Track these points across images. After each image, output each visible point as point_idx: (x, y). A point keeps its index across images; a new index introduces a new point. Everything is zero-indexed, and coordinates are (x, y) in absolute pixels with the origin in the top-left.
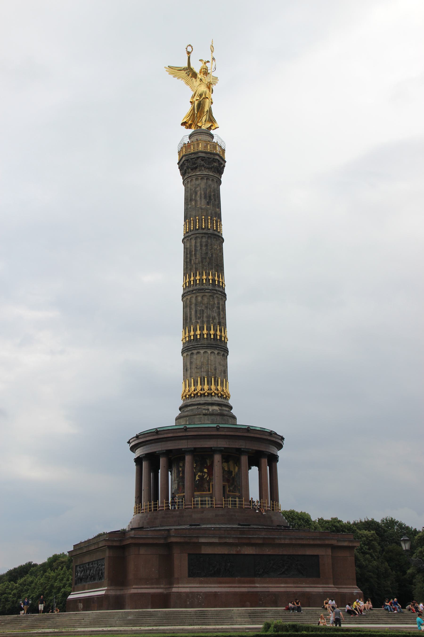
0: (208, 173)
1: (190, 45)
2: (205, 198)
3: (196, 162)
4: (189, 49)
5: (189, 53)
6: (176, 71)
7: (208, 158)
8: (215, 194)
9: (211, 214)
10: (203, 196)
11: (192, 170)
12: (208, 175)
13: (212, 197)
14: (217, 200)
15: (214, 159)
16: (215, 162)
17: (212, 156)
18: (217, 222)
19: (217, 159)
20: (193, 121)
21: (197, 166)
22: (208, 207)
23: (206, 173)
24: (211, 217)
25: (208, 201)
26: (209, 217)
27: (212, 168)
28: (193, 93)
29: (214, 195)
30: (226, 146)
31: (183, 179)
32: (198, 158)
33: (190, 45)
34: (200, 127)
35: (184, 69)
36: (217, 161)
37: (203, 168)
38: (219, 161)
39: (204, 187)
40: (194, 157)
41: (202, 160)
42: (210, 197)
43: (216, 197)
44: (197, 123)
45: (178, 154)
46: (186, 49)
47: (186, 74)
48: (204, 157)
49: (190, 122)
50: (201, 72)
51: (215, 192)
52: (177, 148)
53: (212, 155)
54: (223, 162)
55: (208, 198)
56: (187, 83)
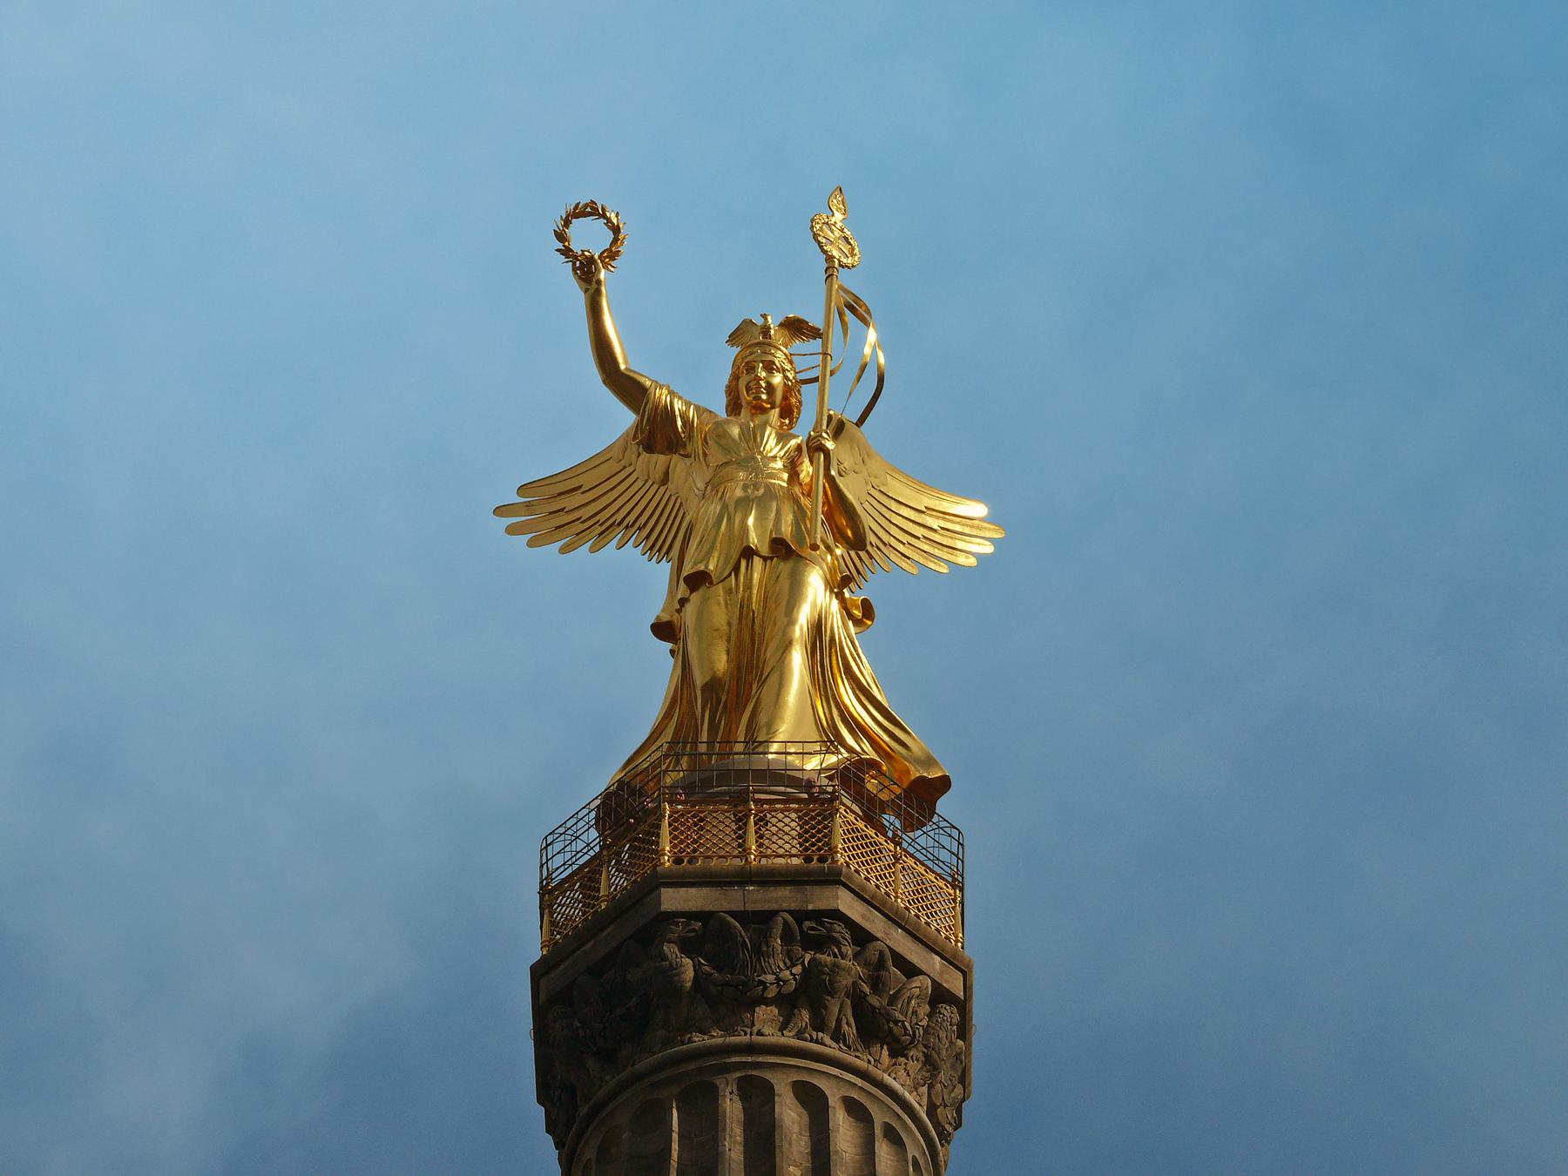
1: (590, 210)
4: (589, 237)
5: (586, 270)
12: (751, 1049)
15: (800, 916)
19: (837, 915)
33: (590, 210)
36: (839, 927)
38: (862, 937)
46: (561, 236)
48: (704, 916)
50: (734, 407)
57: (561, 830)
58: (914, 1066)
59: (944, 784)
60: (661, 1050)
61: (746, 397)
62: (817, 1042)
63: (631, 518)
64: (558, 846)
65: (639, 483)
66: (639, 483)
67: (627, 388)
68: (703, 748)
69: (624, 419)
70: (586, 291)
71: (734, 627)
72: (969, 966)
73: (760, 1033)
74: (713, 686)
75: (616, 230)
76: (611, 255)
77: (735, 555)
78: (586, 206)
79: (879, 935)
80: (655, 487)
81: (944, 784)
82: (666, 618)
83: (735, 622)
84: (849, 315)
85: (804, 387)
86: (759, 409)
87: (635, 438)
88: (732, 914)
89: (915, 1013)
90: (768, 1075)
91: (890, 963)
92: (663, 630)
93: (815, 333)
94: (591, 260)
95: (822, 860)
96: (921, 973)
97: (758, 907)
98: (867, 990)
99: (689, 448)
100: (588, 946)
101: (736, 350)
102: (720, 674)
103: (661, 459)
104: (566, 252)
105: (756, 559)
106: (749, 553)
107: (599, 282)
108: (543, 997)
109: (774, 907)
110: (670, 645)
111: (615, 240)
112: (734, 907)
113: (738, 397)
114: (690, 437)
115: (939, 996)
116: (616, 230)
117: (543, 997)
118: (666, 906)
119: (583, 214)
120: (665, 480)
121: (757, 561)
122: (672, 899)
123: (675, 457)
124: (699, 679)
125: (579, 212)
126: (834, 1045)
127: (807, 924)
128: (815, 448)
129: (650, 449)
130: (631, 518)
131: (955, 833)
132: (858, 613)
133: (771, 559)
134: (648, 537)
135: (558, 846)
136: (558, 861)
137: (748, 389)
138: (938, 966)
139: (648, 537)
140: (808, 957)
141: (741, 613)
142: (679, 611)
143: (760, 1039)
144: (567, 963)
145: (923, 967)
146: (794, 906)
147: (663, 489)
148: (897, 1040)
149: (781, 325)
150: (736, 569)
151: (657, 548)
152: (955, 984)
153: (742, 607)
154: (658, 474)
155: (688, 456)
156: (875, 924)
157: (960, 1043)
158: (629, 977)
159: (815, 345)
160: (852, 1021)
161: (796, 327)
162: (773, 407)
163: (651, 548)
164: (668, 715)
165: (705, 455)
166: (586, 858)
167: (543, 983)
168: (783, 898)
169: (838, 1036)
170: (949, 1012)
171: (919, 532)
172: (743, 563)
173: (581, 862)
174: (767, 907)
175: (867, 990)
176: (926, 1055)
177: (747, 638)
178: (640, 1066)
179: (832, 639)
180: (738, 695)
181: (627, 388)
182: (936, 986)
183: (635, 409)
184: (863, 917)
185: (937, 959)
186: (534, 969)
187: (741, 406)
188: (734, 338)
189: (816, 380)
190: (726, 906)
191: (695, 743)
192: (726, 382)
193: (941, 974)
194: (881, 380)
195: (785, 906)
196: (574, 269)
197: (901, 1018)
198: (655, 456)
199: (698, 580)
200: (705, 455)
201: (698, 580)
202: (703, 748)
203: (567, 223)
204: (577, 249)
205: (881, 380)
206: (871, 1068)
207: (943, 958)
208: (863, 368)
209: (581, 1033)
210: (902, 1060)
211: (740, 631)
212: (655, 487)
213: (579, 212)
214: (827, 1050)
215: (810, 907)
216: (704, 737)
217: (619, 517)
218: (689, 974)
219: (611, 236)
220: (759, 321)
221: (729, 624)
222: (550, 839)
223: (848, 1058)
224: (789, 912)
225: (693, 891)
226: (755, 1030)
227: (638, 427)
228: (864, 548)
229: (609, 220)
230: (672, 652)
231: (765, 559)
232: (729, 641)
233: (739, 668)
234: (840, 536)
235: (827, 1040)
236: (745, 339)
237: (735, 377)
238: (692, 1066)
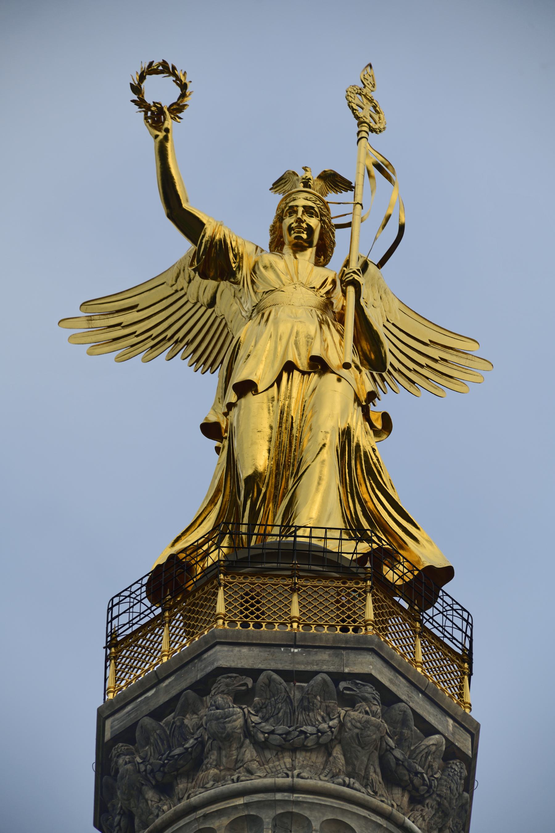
1: (165, 69)
3: (190, 721)
4: (160, 90)
5: (156, 117)
7: (289, 676)
11: (166, 789)
12: (292, 789)
15: (337, 677)
16: (350, 702)
21: (201, 743)
23: (268, 781)
27: (326, 749)
32: (202, 687)
36: (369, 690)
37: (249, 753)
38: (389, 699)
41: (241, 697)
46: (136, 89)
48: (254, 673)
50: (277, 245)
53: (325, 656)
57: (127, 593)
58: (428, 812)
59: (447, 573)
60: (213, 786)
61: (288, 238)
62: (348, 786)
63: (181, 334)
64: (124, 607)
65: (189, 306)
66: (189, 306)
67: (188, 224)
68: (244, 529)
69: (181, 247)
70: (156, 137)
71: (276, 429)
72: (477, 726)
73: (299, 776)
74: (254, 479)
75: (183, 87)
76: (177, 109)
77: (278, 366)
78: (160, 64)
79: (403, 697)
80: (203, 309)
81: (447, 573)
82: (213, 419)
83: (276, 426)
84: (375, 172)
85: (338, 232)
86: (299, 247)
87: (191, 265)
88: (277, 671)
89: (430, 767)
90: (307, 813)
91: (412, 723)
92: (210, 430)
93: (348, 186)
94: (161, 111)
95: (356, 630)
96: (437, 732)
97: (302, 668)
98: (392, 743)
99: (239, 276)
100: (150, 694)
101: (279, 197)
102: (261, 469)
103: (211, 284)
104: (141, 103)
105: (296, 373)
106: (289, 367)
107: (167, 130)
108: (108, 736)
109: (315, 668)
110: (216, 443)
111: (183, 96)
112: (280, 667)
113: (281, 236)
114: (239, 268)
115: (452, 753)
116: (183, 87)
117: (108, 736)
118: (223, 663)
119: (156, 72)
120: (212, 303)
121: (296, 373)
123: (224, 284)
124: (245, 472)
125: (151, 70)
126: (363, 790)
128: (348, 282)
129: (204, 276)
130: (181, 334)
131: (465, 615)
132: (379, 425)
133: (309, 374)
134: (194, 351)
135: (124, 607)
136: (124, 619)
137: (290, 229)
138: (451, 728)
139: (194, 351)
140: (343, 712)
141: (281, 418)
142: (226, 414)
143: (301, 781)
144: (129, 708)
145: (440, 728)
146: (332, 669)
147: (210, 311)
148: (417, 789)
149: (320, 177)
150: (279, 380)
151: (205, 361)
152: (463, 743)
153: (282, 413)
154: (205, 299)
155: (237, 283)
156: (400, 688)
157: (466, 795)
158: (186, 721)
159: (346, 196)
160: (378, 770)
161: (334, 181)
162: (311, 246)
163: (197, 361)
164: (213, 502)
165: (253, 282)
166: (147, 619)
167: (108, 723)
168: (324, 661)
169: (366, 783)
170: (457, 766)
171: (423, 360)
172: (285, 376)
173: (143, 622)
174: (309, 668)
175: (392, 743)
176: (439, 804)
177: (285, 438)
178: (194, 800)
179: (358, 446)
180: (276, 487)
181: (188, 224)
182: (450, 744)
183: (194, 242)
184: (391, 681)
185: (451, 722)
186: (100, 711)
187: (283, 244)
188: (278, 185)
189: (349, 225)
190: (273, 666)
191: (238, 524)
192: (271, 223)
193: (453, 734)
194: (402, 228)
195: (325, 668)
196: (146, 118)
197: (420, 769)
198: (206, 282)
199: (246, 388)
200: (253, 282)
201: (246, 388)
202: (244, 529)
203: (142, 78)
204: (149, 99)
205: (402, 228)
206: (395, 811)
207: (455, 720)
208: (388, 218)
209: (142, 768)
210: (419, 807)
211: (280, 433)
212: (203, 309)
213: (151, 70)
214: (358, 794)
215: (346, 670)
216: (246, 520)
217: (169, 333)
218: (240, 722)
219: (178, 91)
220: (301, 174)
221: (271, 428)
222: (116, 600)
223: (376, 801)
224: (329, 673)
225: (245, 650)
226: (296, 772)
227: (196, 254)
228: (384, 368)
229: (177, 78)
230: (218, 450)
231: (303, 373)
232: (270, 441)
233: (278, 465)
234: (366, 360)
235: (357, 785)
236: (287, 187)
237: (280, 218)
238: (240, 801)
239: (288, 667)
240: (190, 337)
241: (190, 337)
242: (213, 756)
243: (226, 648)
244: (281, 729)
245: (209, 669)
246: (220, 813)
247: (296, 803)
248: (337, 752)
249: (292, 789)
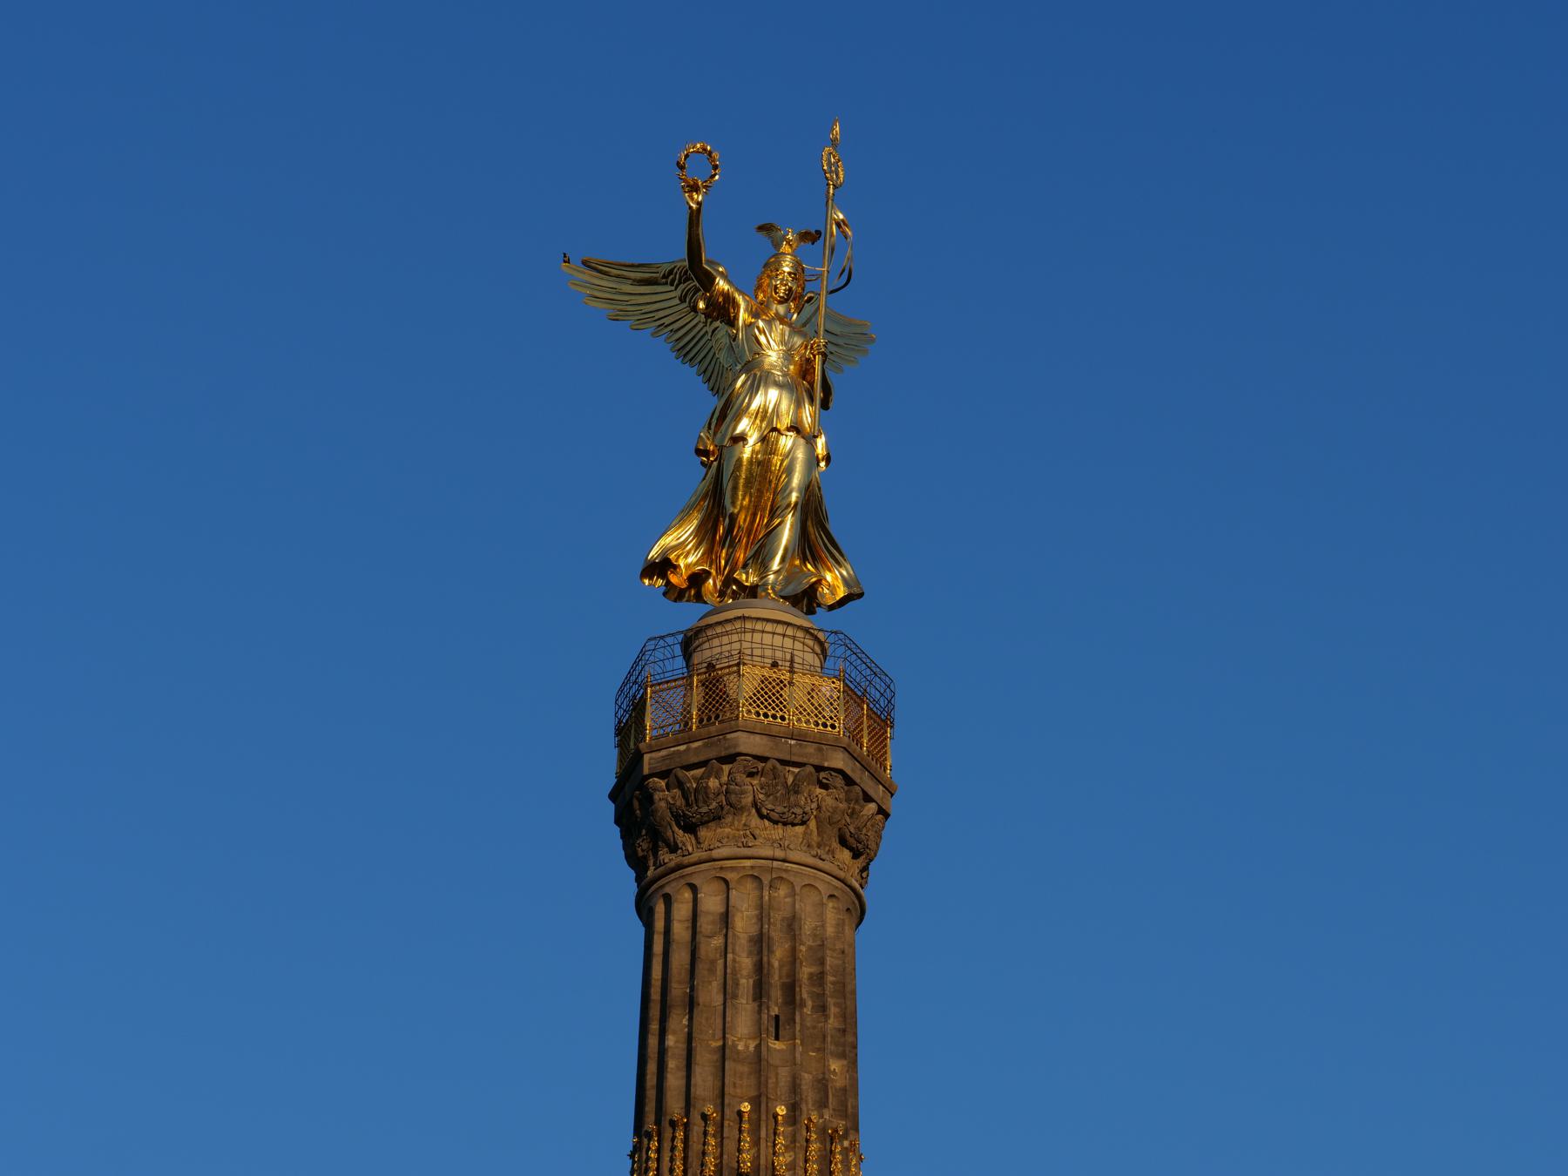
0: (779, 853)
2: (760, 992)
3: (713, 783)
6: (628, 288)
8: (822, 975)
9: (795, 1087)
10: (746, 983)
13: (805, 993)
14: (833, 1010)
15: (819, 769)
17: (810, 753)
18: (828, 1138)
20: (710, 556)
22: (778, 1045)
23: (768, 852)
24: (794, 1108)
25: (775, 1011)
26: (781, 1110)
28: (716, 403)
29: (818, 979)
30: (897, 701)
31: (639, 879)
34: (753, 592)
35: (669, 277)
36: (839, 781)
37: (755, 821)
38: (849, 781)
39: (754, 930)
40: (702, 758)
42: (790, 989)
43: (829, 988)
44: (732, 571)
45: (610, 739)
46: (682, 168)
47: (682, 299)
48: (764, 759)
49: (689, 560)
51: (822, 962)
52: (612, 708)
54: (877, 792)
55: (776, 994)
56: (686, 351)
63: (667, 321)
100: (682, 748)
112: (781, 756)
122: (748, 743)
127: (822, 775)
144: (664, 753)
146: (816, 762)
218: (750, 799)
222: (651, 646)
225: (758, 737)
238: (748, 863)
239: (787, 758)
240: (675, 326)
241: (675, 326)
242: (729, 819)
243: (745, 735)
244: (779, 809)
245: (732, 751)
246: (733, 869)
247: (786, 871)
248: (813, 824)
249: (784, 861)
